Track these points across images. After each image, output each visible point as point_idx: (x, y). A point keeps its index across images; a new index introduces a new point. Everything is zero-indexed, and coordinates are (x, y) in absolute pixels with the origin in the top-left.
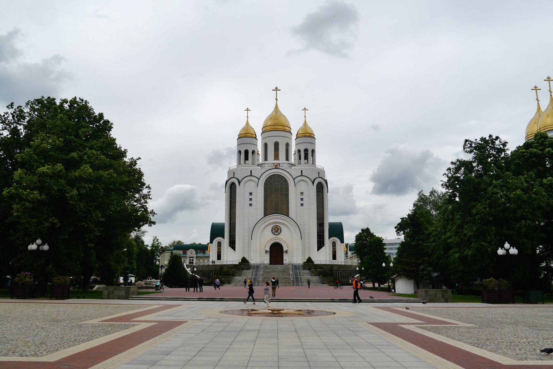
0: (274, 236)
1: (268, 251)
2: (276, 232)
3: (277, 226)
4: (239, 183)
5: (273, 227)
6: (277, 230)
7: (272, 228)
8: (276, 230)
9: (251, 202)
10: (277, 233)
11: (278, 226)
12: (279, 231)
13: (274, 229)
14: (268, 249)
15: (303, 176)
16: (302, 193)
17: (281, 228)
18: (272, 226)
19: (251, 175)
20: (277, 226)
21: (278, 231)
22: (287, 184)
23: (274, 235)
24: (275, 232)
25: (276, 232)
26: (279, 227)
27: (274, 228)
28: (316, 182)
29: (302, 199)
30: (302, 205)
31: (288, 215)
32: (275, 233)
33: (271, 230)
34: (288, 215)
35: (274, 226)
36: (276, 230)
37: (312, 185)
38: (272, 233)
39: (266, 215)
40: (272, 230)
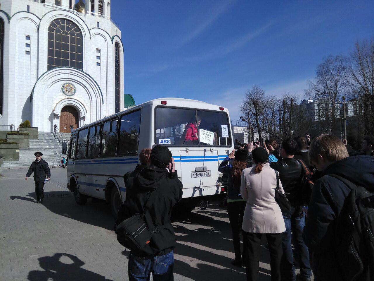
0: (64, 97)
1: (58, 115)
2: (69, 92)
3: (70, 85)
4: (9, 18)
5: (65, 84)
6: (69, 89)
7: (63, 86)
8: (68, 90)
9: (28, 49)
10: (70, 94)
11: (71, 84)
12: (73, 91)
13: (66, 87)
14: (58, 112)
15: (100, 29)
16: (98, 50)
17: (75, 87)
18: (62, 83)
19: (28, 11)
20: (70, 85)
21: (70, 90)
22: (81, 35)
23: (66, 96)
24: (67, 92)
25: (69, 92)
26: (73, 85)
27: (66, 86)
28: (114, 42)
29: (98, 57)
30: (98, 64)
31: (82, 71)
32: (67, 93)
33: (61, 88)
34: (82, 71)
35: (66, 83)
36: (68, 89)
37: (112, 43)
38: (62, 92)
39: (50, 68)
40: (63, 89)
